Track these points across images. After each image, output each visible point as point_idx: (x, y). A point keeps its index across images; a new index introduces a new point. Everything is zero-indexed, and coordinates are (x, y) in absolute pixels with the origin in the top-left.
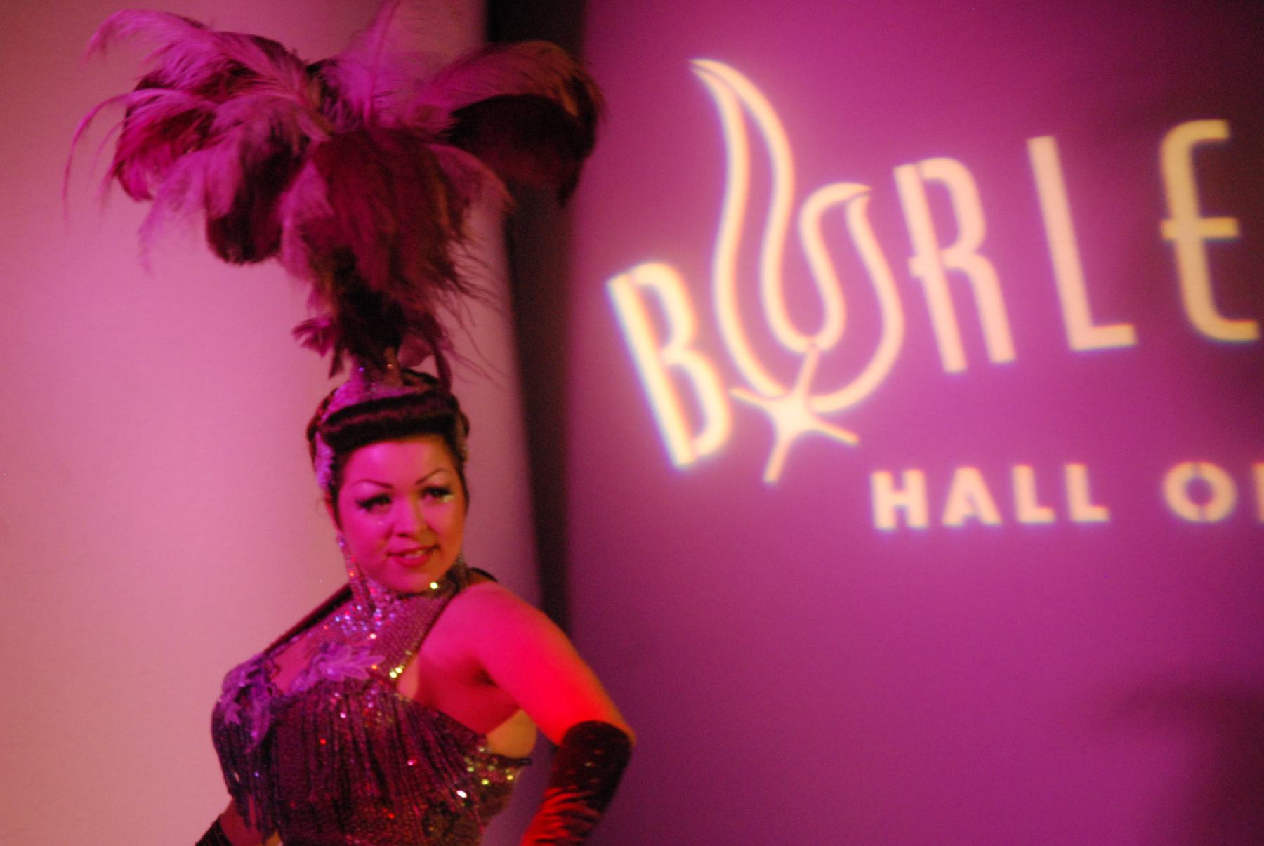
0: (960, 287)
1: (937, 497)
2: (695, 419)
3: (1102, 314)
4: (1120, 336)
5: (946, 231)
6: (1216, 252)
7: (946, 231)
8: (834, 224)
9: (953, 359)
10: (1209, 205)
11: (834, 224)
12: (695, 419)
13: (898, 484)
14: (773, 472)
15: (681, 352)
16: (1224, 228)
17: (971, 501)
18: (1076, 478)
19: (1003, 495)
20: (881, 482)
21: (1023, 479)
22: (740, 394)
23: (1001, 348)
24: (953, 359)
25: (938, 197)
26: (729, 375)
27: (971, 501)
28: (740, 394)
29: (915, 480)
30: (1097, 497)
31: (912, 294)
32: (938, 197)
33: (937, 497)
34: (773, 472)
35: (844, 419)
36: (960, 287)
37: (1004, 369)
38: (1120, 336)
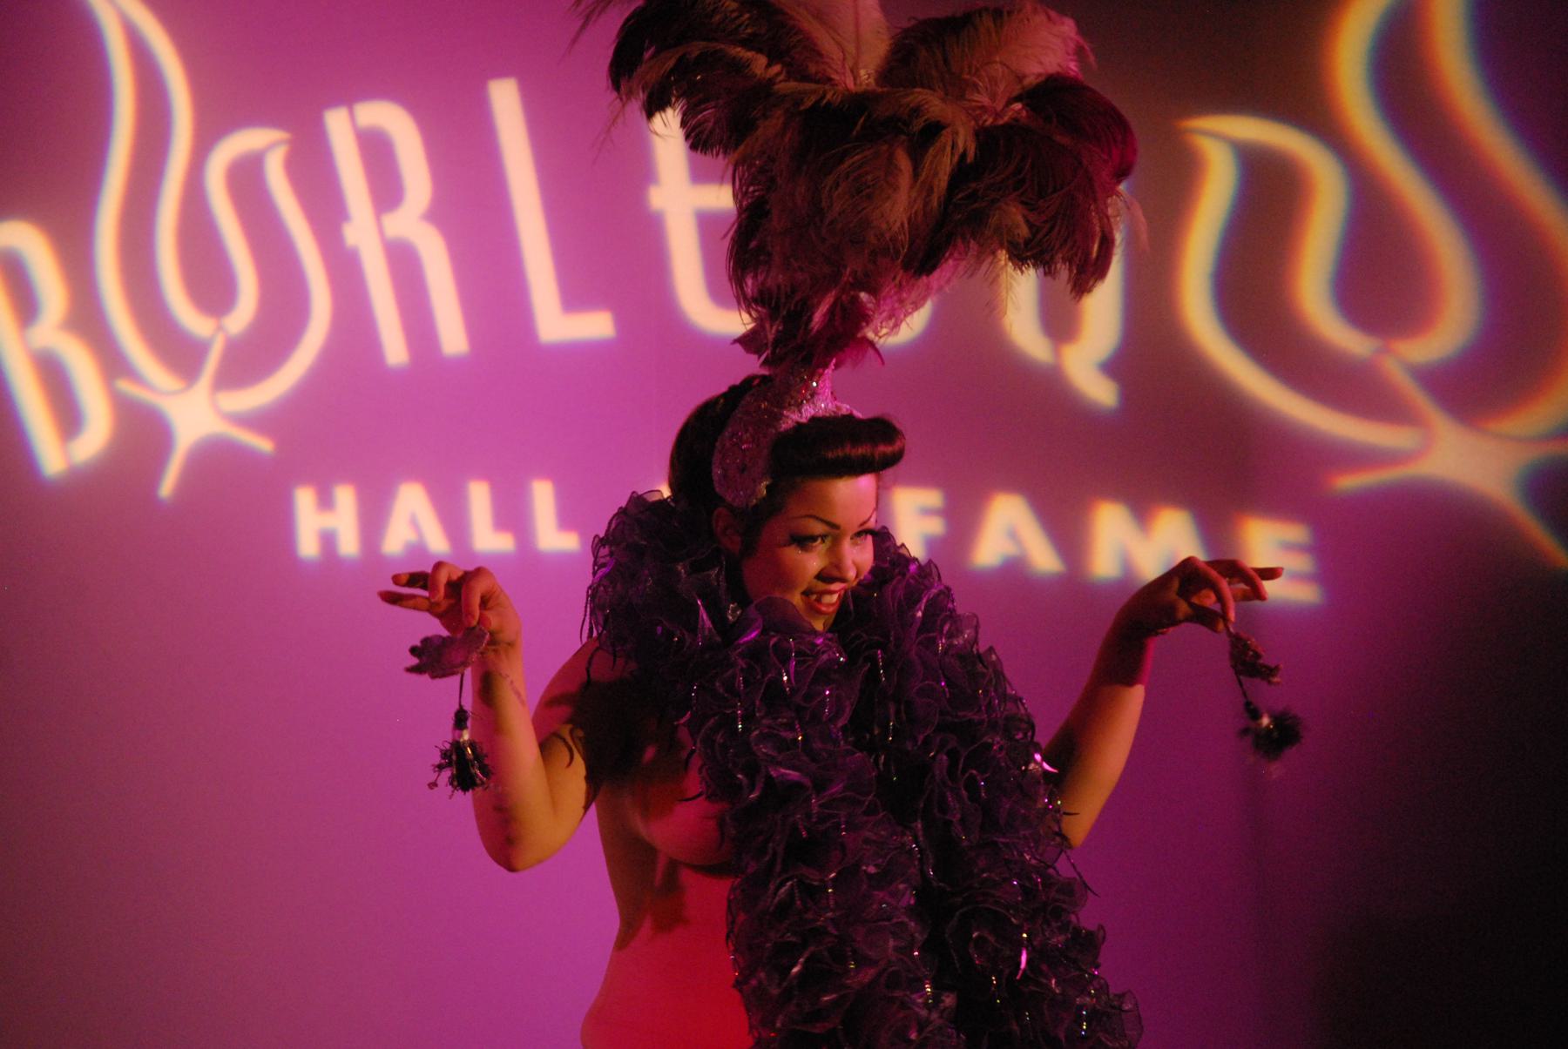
0: (403, 261)
1: (373, 519)
3: (574, 298)
4: (596, 326)
5: (387, 191)
7: (387, 191)
8: (246, 178)
11: (246, 178)
12: (69, 418)
13: (325, 502)
14: (167, 487)
15: (51, 331)
17: (414, 524)
18: (543, 497)
19: (454, 518)
20: (304, 499)
21: (479, 497)
22: (125, 386)
23: (453, 337)
24: (395, 349)
25: (376, 149)
26: (113, 363)
27: (414, 524)
28: (125, 386)
29: (345, 497)
30: (566, 520)
31: (344, 269)
32: (376, 149)
33: (373, 519)
34: (167, 487)
35: (257, 421)
36: (403, 261)
37: (458, 363)
38: (596, 326)
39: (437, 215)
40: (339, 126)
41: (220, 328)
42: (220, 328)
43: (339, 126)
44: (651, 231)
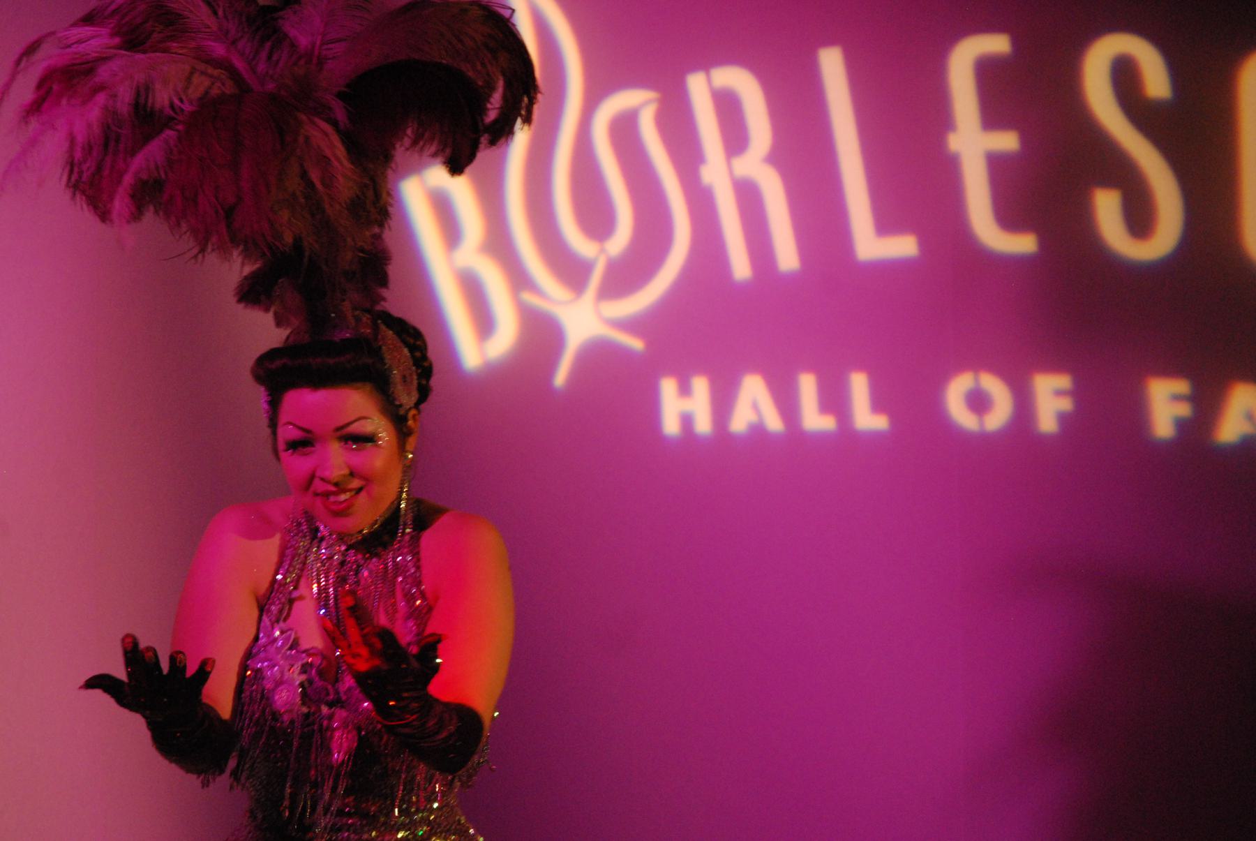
0: (748, 195)
1: (723, 403)
2: (484, 323)
3: (885, 225)
4: (904, 246)
5: (736, 139)
6: (997, 164)
7: (736, 139)
8: (624, 130)
9: (741, 267)
10: (992, 118)
11: (624, 130)
12: (484, 323)
13: (685, 390)
14: (561, 377)
16: (1007, 141)
17: (755, 407)
18: (859, 386)
19: (787, 403)
20: (668, 388)
21: (808, 386)
22: (528, 297)
23: (787, 256)
24: (741, 267)
25: (727, 105)
26: (519, 279)
27: (755, 407)
28: (528, 297)
29: (701, 386)
30: (878, 405)
31: (701, 202)
32: (727, 105)
33: (723, 403)
34: (561, 377)
35: (631, 325)
36: (748, 195)
37: (791, 278)
38: (904, 246)
39: (776, 158)
40: (698, 87)
41: (602, 250)
42: (602, 250)
43: (698, 87)
44: (949, 168)
